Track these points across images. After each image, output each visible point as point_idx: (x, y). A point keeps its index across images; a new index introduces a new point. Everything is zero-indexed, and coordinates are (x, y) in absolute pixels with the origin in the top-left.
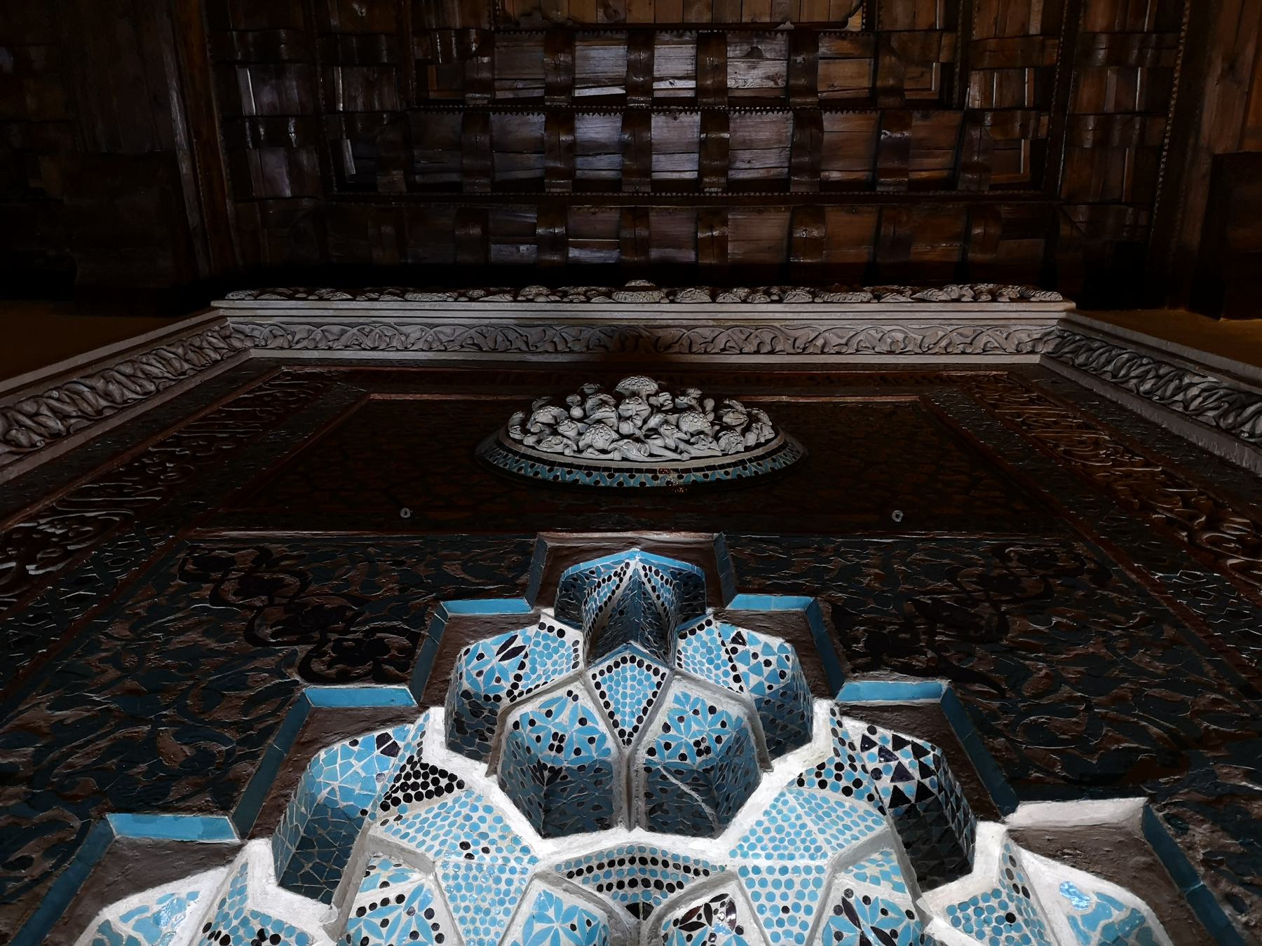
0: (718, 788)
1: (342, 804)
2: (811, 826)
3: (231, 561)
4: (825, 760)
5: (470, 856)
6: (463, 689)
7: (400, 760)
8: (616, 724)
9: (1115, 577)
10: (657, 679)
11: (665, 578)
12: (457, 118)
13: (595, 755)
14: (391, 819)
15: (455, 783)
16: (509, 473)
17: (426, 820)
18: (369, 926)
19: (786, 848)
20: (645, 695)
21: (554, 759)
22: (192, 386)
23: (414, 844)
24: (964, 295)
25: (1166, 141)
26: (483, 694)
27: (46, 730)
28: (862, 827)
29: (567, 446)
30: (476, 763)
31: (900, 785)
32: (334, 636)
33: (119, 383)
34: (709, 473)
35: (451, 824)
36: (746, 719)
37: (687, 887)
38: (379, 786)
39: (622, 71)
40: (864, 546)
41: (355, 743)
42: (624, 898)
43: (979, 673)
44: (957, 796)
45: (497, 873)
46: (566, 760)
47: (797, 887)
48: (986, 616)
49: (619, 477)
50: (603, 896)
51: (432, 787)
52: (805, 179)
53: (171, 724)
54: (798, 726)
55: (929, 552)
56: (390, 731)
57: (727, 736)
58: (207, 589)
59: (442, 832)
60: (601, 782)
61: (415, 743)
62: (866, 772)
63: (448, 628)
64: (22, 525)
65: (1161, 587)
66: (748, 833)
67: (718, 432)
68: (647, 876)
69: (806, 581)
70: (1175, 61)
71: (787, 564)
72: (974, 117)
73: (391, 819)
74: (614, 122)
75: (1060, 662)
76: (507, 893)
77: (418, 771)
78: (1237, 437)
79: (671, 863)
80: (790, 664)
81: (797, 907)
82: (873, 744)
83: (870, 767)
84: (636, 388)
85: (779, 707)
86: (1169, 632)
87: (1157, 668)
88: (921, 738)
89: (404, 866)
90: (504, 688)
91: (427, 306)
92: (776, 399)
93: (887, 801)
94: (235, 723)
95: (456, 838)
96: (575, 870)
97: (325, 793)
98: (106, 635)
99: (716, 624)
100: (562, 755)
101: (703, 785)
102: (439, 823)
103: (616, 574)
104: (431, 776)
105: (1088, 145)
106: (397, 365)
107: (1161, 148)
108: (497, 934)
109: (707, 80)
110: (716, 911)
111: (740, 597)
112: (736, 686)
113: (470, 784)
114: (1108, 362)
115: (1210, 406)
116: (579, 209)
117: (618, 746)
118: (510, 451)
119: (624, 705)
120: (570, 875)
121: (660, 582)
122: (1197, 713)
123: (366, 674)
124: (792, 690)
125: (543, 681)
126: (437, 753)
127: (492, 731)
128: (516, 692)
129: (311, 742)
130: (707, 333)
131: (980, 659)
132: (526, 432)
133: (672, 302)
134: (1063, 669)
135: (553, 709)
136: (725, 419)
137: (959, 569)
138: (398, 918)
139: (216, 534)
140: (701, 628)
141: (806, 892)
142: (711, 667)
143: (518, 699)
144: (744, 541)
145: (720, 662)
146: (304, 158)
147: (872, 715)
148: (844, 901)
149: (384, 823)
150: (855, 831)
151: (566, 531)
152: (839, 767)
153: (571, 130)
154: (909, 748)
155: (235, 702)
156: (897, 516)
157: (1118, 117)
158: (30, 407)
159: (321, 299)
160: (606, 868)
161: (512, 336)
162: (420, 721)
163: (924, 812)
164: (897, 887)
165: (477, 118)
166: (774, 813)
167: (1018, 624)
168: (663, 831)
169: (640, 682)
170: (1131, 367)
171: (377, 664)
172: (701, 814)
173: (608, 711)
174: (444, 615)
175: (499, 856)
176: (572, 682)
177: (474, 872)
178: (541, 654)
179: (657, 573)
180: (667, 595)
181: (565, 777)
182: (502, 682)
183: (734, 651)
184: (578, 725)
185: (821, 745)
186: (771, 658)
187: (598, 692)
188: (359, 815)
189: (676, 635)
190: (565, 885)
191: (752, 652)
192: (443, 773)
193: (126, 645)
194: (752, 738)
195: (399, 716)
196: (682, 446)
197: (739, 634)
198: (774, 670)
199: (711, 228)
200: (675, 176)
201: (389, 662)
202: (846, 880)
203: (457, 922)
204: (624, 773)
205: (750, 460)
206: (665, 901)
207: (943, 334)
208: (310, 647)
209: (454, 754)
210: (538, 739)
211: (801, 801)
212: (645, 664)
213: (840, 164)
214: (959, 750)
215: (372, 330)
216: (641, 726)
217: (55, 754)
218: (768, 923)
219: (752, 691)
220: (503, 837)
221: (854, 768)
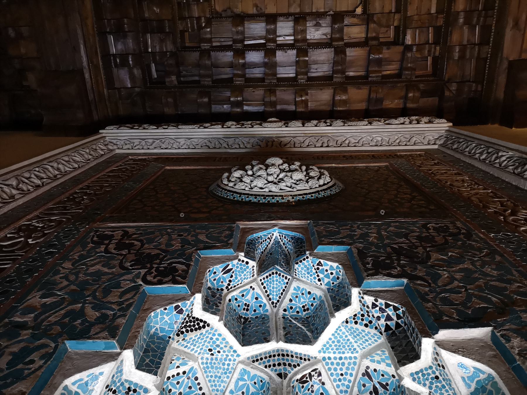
0: (313, 325)
1: (161, 334)
2: (352, 340)
4: (357, 313)
5: (212, 354)
6: (208, 286)
7: (184, 316)
8: (270, 299)
9: (474, 236)
10: (286, 281)
11: (289, 239)
13: (262, 312)
14: (181, 340)
15: (206, 325)
17: (195, 340)
18: (172, 384)
19: (341, 349)
20: (282, 287)
21: (246, 314)
23: (190, 350)
25: (489, 55)
26: (216, 288)
28: (373, 340)
29: (246, 186)
30: (215, 316)
31: (389, 323)
32: (155, 266)
34: (305, 196)
35: (205, 341)
36: (323, 296)
37: (301, 366)
38: (175, 326)
39: (264, 33)
40: (370, 225)
41: (165, 309)
42: (276, 370)
43: (420, 276)
44: (413, 327)
45: (223, 361)
46: (250, 314)
47: (346, 365)
48: (421, 253)
50: (268, 370)
51: (197, 327)
52: (339, 75)
54: (346, 299)
56: (180, 304)
57: (316, 304)
58: (103, 248)
59: (201, 345)
60: (265, 323)
61: (189, 309)
62: (374, 317)
66: (325, 343)
67: (308, 179)
68: (285, 361)
71: (338, 233)
72: (408, 48)
73: (181, 340)
75: (453, 271)
76: (228, 369)
77: (191, 320)
79: (294, 356)
80: (341, 274)
81: (346, 374)
82: (377, 306)
83: (376, 315)
84: (273, 162)
85: (337, 291)
86: (498, 258)
88: (397, 303)
89: (186, 359)
92: (330, 165)
93: (383, 329)
94: (116, 302)
95: (207, 347)
96: (255, 359)
97: (153, 330)
98: (62, 267)
99: (310, 258)
100: (248, 312)
101: (306, 324)
102: (200, 341)
103: (268, 238)
104: (196, 322)
105: (456, 58)
107: (487, 58)
108: (224, 386)
110: (313, 376)
112: (319, 283)
113: (212, 324)
117: (271, 308)
118: (223, 189)
119: (273, 292)
120: (254, 361)
121: (286, 241)
123: (169, 281)
124: (342, 284)
125: (240, 282)
126: (199, 312)
127: (220, 303)
128: (229, 287)
129: (147, 309)
130: (302, 139)
131: (419, 270)
133: (287, 127)
135: (245, 294)
136: (310, 174)
138: (184, 380)
140: (304, 259)
141: (350, 367)
142: (309, 275)
144: (320, 224)
145: (312, 273)
147: (376, 294)
148: (366, 371)
149: (177, 342)
150: (370, 342)
151: (248, 221)
152: (363, 315)
154: (392, 307)
155: (116, 293)
156: (382, 212)
157: (468, 46)
160: (268, 358)
162: (192, 299)
163: (399, 333)
164: (388, 365)
166: (336, 335)
167: (435, 256)
168: (291, 343)
169: (280, 282)
171: (174, 276)
172: (306, 335)
173: (267, 294)
174: (200, 256)
175: (224, 354)
176: (252, 283)
177: (214, 361)
180: (289, 247)
181: (250, 321)
182: (224, 283)
183: (318, 269)
184: (255, 300)
185: (355, 307)
186: (333, 271)
187: (262, 286)
188: (168, 338)
189: (294, 263)
190: (251, 366)
191: (325, 269)
192: (201, 321)
193: (70, 271)
194: (326, 304)
196: (293, 185)
197: (320, 262)
198: (335, 276)
199: (301, 96)
201: (179, 276)
202: (366, 362)
203: (207, 382)
204: (274, 319)
205: (321, 191)
206: (292, 372)
208: (146, 270)
209: (205, 313)
210: (239, 306)
211: (347, 330)
212: (282, 275)
213: (353, 69)
214: (413, 308)
218: (335, 380)
219: (326, 285)
220: (226, 346)
221: (369, 316)
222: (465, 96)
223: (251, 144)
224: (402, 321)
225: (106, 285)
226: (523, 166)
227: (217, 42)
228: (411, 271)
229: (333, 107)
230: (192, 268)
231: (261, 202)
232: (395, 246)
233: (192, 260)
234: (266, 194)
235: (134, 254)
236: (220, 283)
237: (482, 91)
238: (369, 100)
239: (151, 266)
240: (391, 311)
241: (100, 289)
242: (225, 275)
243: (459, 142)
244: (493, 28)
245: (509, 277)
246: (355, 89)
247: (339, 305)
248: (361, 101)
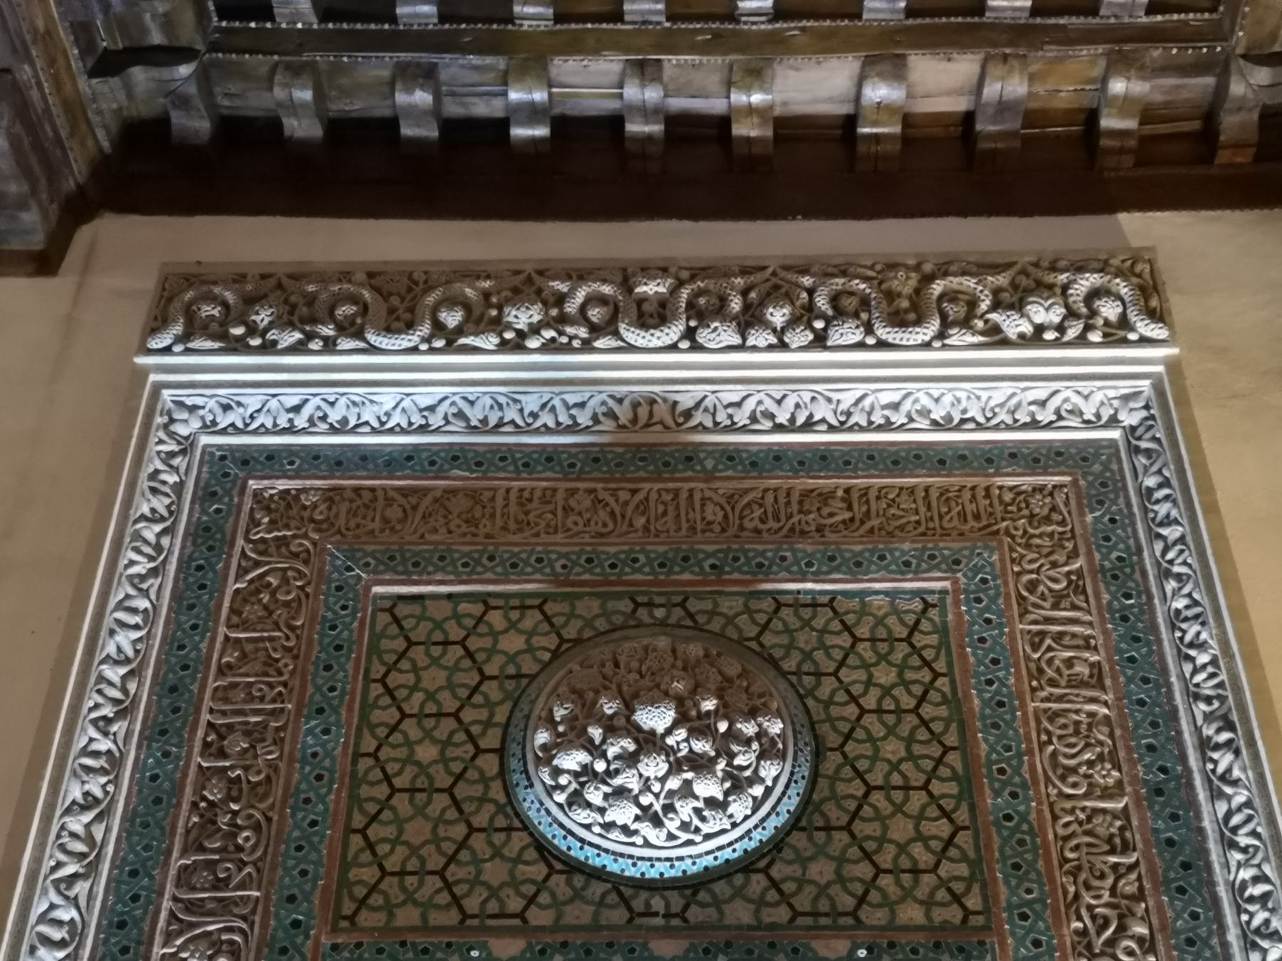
34: (718, 854)
130: (735, 398)
133: (696, 347)
161: (502, 400)
196: (696, 822)
205: (756, 827)
231: (627, 874)
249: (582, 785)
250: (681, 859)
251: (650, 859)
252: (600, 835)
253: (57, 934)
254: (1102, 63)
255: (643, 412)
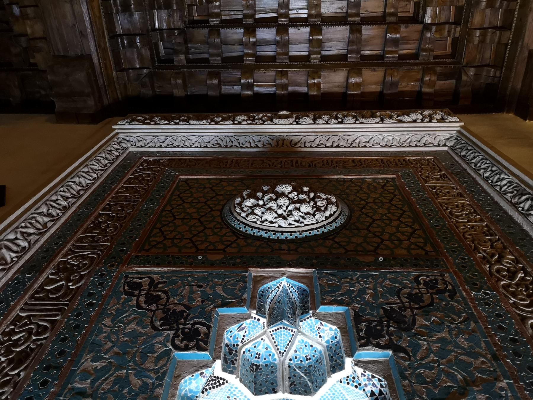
1: (189, 395)
3: (140, 284)
6: (226, 343)
8: (278, 349)
12: (206, 31)
13: (271, 360)
16: (236, 229)
20: (288, 339)
22: (110, 171)
24: (418, 119)
25: (510, 41)
26: (232, 344)
27: (92, 372)
29: (258, 220)
33: (83, 177)
34: (311, 232)
36: (323, 351)
39: (276, 6)
40: (367, 276)
41: (193, 376)
43: (403, 348)
46: (261, 362)
48: (408, 316)
49: (278, 234)
51: (218, 384)
52: (354, 56)
53: (133, 369)
54: (341, 361)
55: (391, 280)
63: (220, 320)
64: (62, 259)
65: (473, 300)
67: (315, 212)
69: (346, 298)
70: (508, 41)
71: (338, 288)
72: (427, 27)
73: (205, 396)
74: (273, 31)
78: (517, 208)
84: (283, 190)
86: (473, 325)
87: (465, 345)
88: (381, 377)
90: (238, 341)
91: (198, 127)
92: (339, 177)
93: (369, 395)
94: (153, 369)
97: (184, 391)
100: (259, 360)
104: (217, 380)
105: (476, 42)
106: (188, 155)
107: (507, 44)
109: (312, 11)
111: (322, 307)
112: (320, 339)
114: (474, 158)
115: (510, 191)
116: (258, 71)
117: (279, 358)
118: (236, 218)
119: (281, 343)
122: (476, 369)
123: (194, 347)
127: (236, 360)
128: (243, 341)
129: (178, 376)
130: (312, 138)
131: (404, 340)
132: (242, 209)
133: (298, 123)
134: (432, 345)
135: (256, 345)
136: (318, 204)
137: (401, 289)
139: (133, 269)
140: (308, 318)
142: (311, 332)
143: (244, 343)
145: (314, 331)
146: (143, 51)
152: (354, 378)
153: (255, 36)
156: (381, 259)
157: (490, 30)
158: (54, 198)
159: (156, 124)
161: (233, 139)
165: (215, 30)
166: (332, 389)
167: (421, 321)
168: (295, 394)
169: (286, 335)
170: (482, 163)
171: (198, 341)
172: (306, 386)
174: (218, 315)
176: (262, 336)
178: (252, 328)
179: (292, 287)
181: (261, 369)
184: (265, 350)
187: (272, 337)
188: (195, 398)
192: (221, 379)
193: (111, 330)
195: (206, 365)
196: (301, 220)
199: (314, 79)
200: (299, 54)
204: (281, 369)
205: (327, 224)
207: (408, 137)
213: (369, 48)
214: (393, 383)
215: (177, 138)
216: (287, 350)
217: (97, 384)
222: (482, 81)
223: (262, 143)
224: (384, 390)
225: (143, 349)
226: (520, 196)
227: (226, 15)
228: (397, 340)
229: (347, 90)
230: (212, 330)
231: (271, 238)
232: (387, 307)
233: (212, 321)
234: (275, 229)
235: (162, 311)
236: (236, 340)
237: (500, 77)
238: (384, 82)
239: (178, 326)
240: (376, 381)
241: (138, 354)
242: (239, 332)
243: (467, 149)
244: (516, 13)
245: (477, 349)
246: (370, 71)
247: (335, 367)
248: (376, 84)
249: (253, 210)
250: (295, 232)
251: (281, 232)
252: (260, 224)
253: (15, 248)
254: (421, 72)
255: (280, 143)
